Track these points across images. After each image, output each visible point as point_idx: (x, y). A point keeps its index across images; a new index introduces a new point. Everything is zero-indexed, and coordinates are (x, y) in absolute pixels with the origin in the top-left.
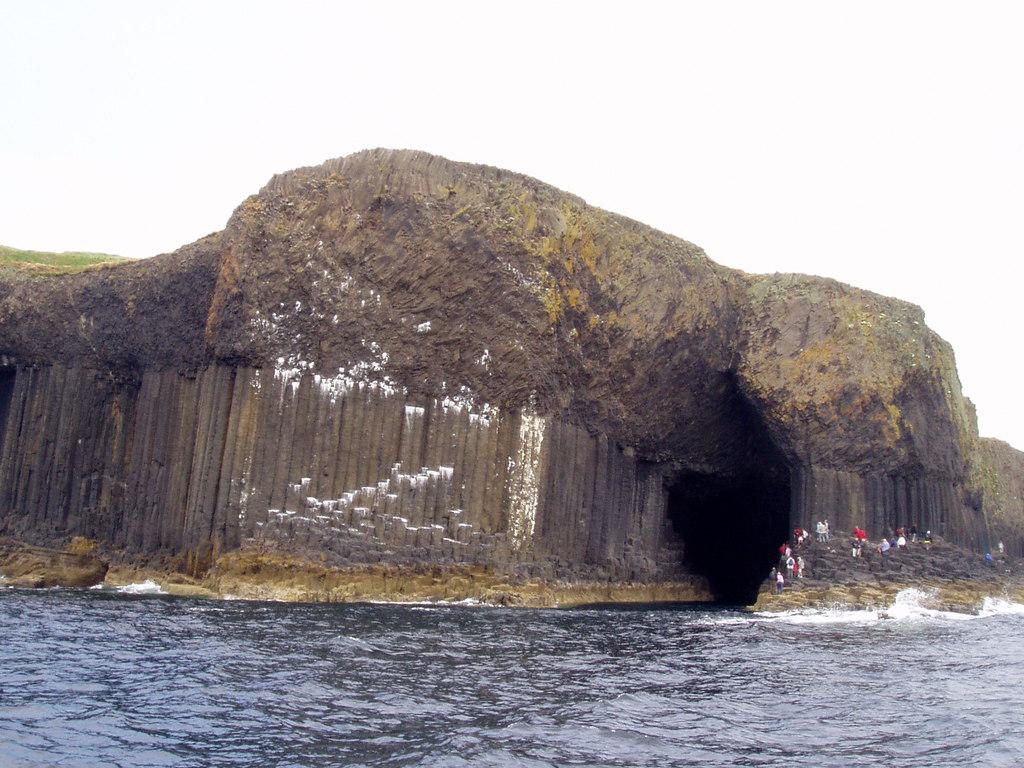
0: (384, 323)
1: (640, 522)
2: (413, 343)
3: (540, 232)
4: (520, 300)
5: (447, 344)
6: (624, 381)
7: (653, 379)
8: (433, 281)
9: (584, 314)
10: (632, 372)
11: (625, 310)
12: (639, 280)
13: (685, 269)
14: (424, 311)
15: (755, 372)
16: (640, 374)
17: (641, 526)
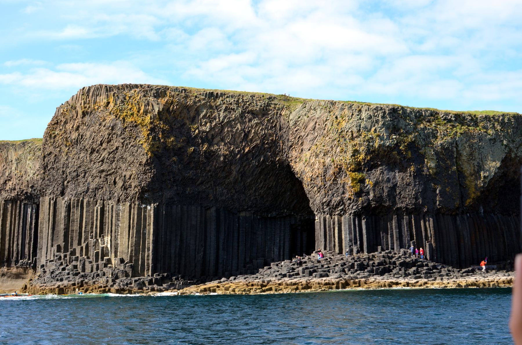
0: (88, 169)
1: (274, 251)
2: (98, 176)
3: (146, 112)
4: (136, 149)
5: (110, 175)
6: (226, 177)
7: (243, 174)
8: (104, 145)
9: (180, 148)
10: (230, 173)
11: (215, 141)
12: (219, 124)
13: (252, 112)
14: (102, 161)
15: (296, 162)
16: (234, 173)
17: (274, 253)
